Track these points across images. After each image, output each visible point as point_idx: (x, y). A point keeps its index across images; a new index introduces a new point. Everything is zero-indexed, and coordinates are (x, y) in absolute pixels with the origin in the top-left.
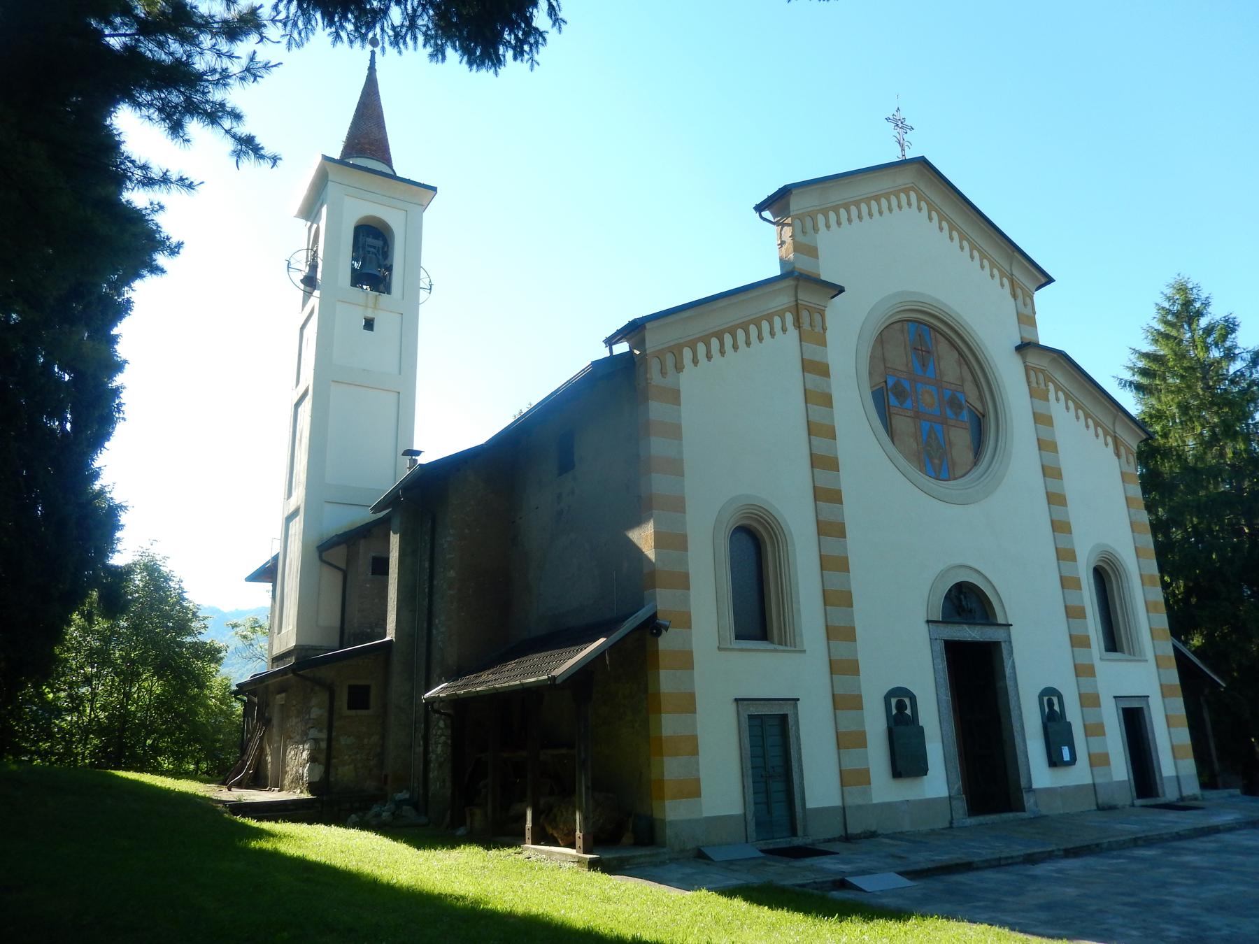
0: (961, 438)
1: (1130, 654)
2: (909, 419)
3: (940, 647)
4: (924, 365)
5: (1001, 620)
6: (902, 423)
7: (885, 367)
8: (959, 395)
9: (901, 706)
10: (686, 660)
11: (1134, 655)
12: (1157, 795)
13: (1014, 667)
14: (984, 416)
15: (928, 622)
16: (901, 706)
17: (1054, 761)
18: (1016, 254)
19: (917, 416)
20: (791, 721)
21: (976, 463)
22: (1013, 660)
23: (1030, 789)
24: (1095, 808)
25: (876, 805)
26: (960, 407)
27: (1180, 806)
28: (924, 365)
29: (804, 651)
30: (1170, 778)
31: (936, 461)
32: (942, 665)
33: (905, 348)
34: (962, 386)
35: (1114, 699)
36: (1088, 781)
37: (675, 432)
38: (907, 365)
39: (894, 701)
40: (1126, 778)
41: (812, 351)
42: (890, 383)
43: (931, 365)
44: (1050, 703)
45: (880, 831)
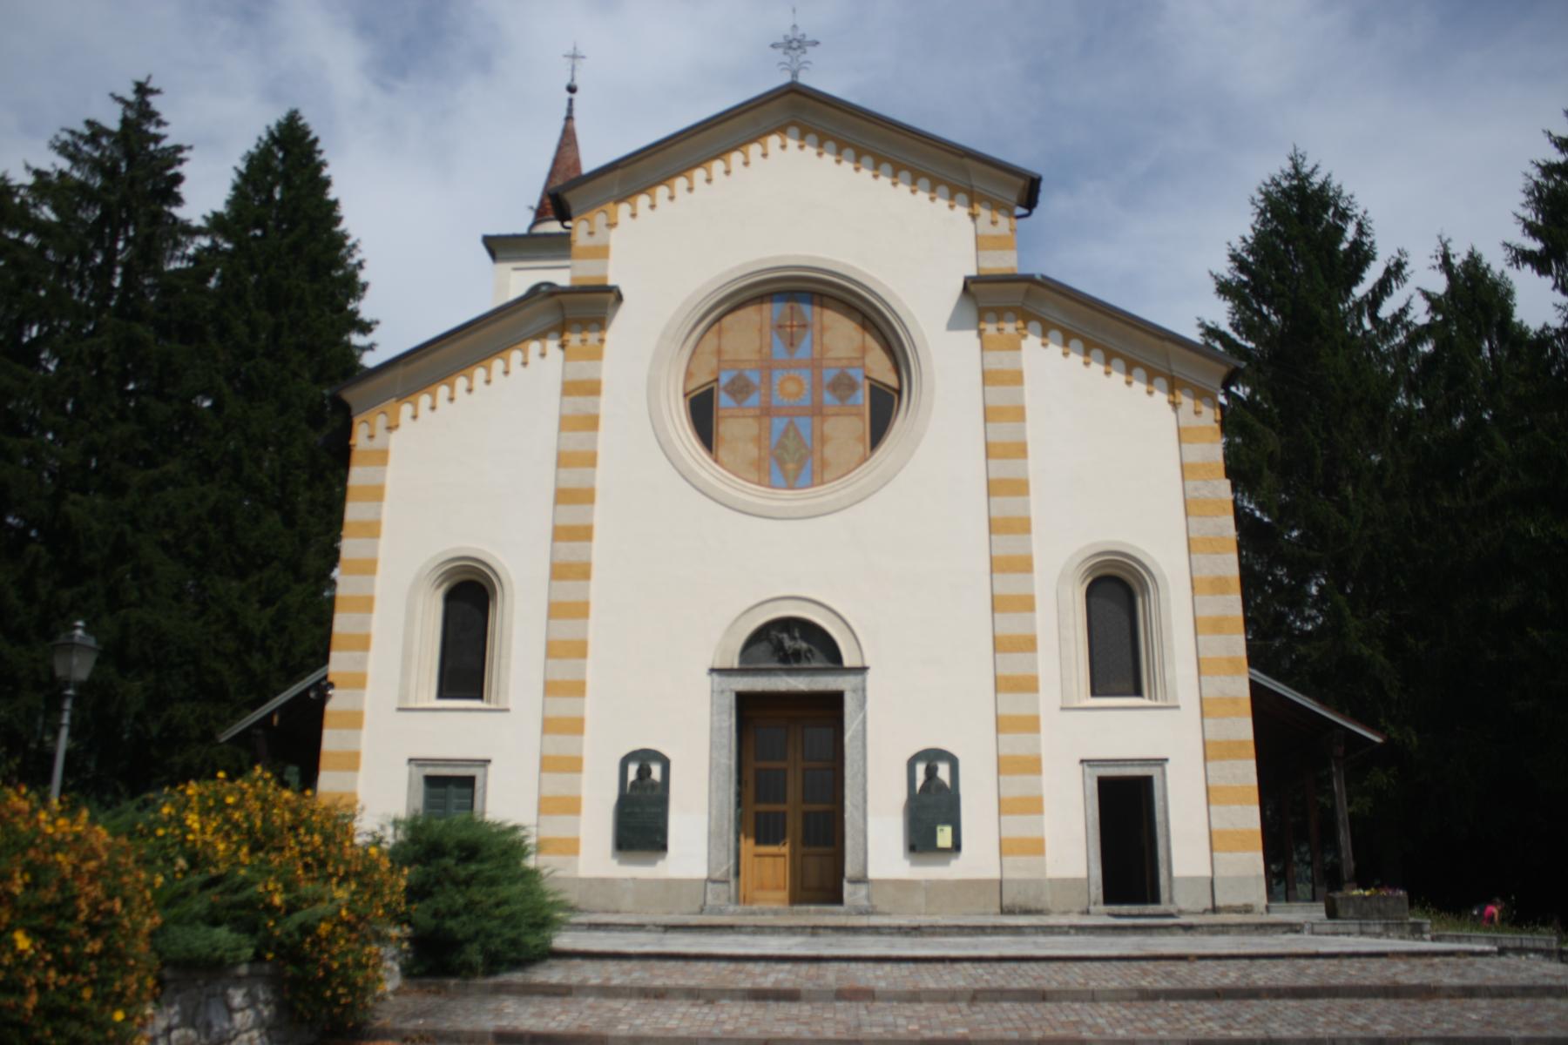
0: (850, 427)
1: (1150, 698)
2: (750, 421)
3: (730, 700)
4: (792, 345)
5: (849, 660)
6: (733, 426)
7: (719, 361)
8: (852, 372)
9: (644, 773)
10: (355, 720)
11: (1156, 699)
12: (1155, 899)
13: (864, 722)
14: (899, 392)
15: (713, 671)
16: (644, 773)
17: (920, 842)
18: (967, 162)
19: (767, 412)
20: (478, 784)
21: (865, 459)
22: (865, 718)
23: (862, 880)
24: (998, 910)
25: (582, 880)
26: (852, 386)
27: (1217, 917)
28: (792, 345)
29: (507, 710)
30: (1193, 880)
31: (791, 466)
32: (729, 721)
33: (760, 330)
34: (863, 358)
35: (1080, 768)
36: (993, 873)
37: (377, 493)
38: (760, 351)
39: (633, 769)
40: (1082, 874)
41: (582, 370)
42: (725, 379)
43: (806, 342)
44: (931, 773)
45: (582, 906)
